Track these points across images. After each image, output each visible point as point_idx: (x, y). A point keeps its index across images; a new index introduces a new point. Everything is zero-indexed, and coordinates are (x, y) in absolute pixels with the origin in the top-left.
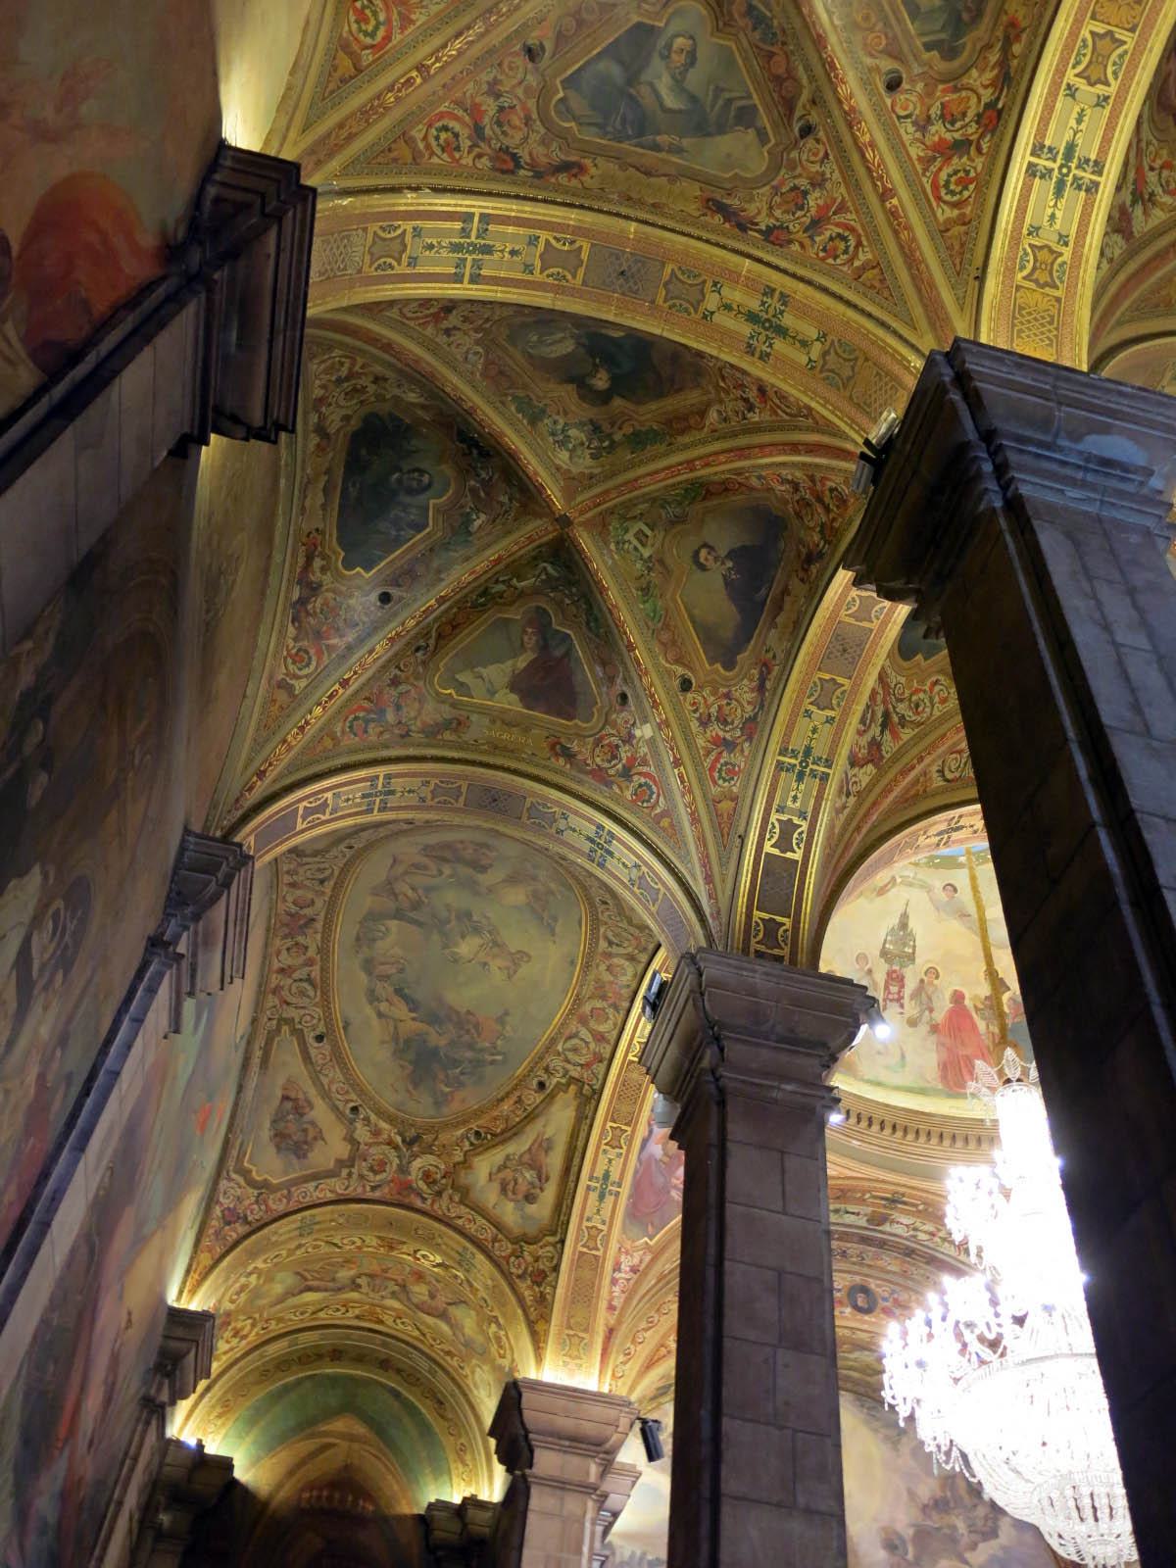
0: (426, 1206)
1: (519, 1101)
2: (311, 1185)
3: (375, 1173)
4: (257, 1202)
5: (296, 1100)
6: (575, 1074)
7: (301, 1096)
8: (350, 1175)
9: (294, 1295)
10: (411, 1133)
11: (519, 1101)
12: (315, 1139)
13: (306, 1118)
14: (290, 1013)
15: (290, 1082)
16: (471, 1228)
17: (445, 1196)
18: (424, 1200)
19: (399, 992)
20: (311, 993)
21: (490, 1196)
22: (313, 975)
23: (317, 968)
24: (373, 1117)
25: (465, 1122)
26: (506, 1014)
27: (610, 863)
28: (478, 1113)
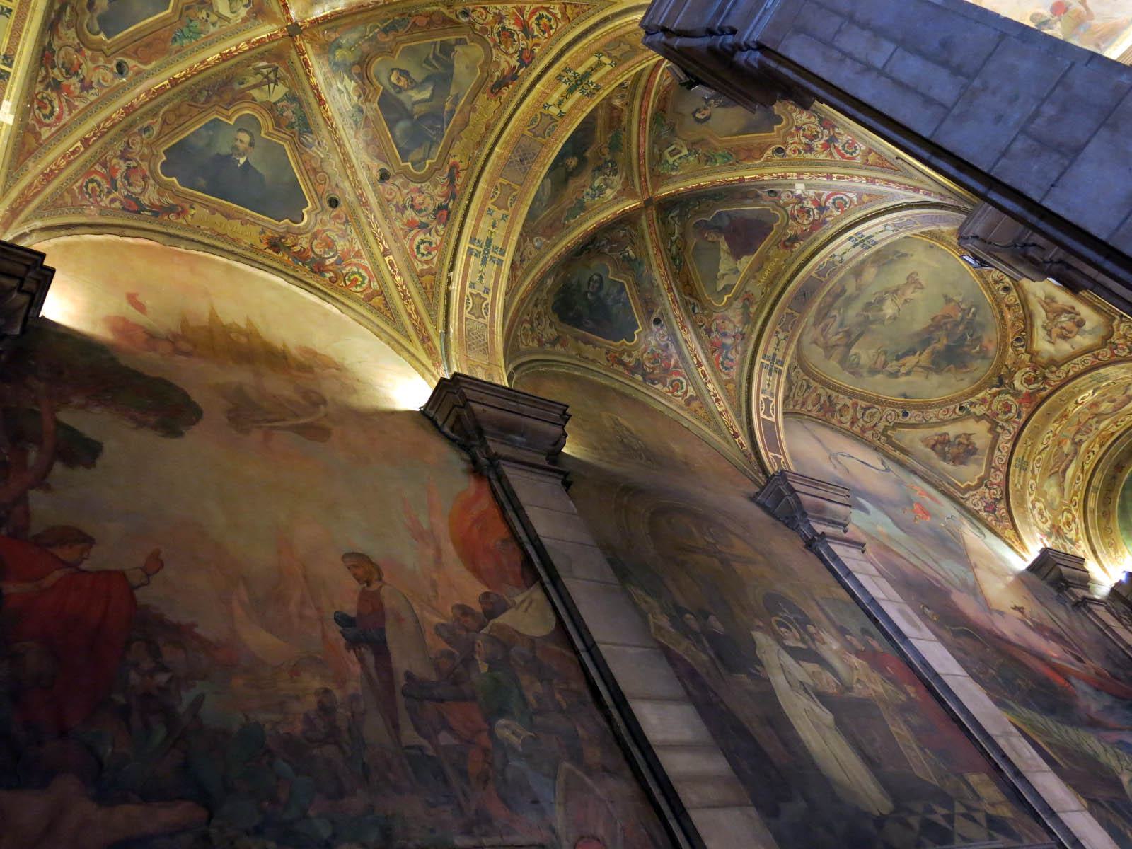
0: (1049, 389)
1: (1009, 307)
2: (997, 453)
3: (1010, 411)
4: (990, 489)
5: (937, 442)
7: (936, 438)
8: (1002, 427)
9: (1064, 481)
10: (995, 380)
11: (1009, 307)
13: (952, 440)
14: (881, 426)
15: (924, 441)
16: (1080, 368)
17: (1049, 375)
18: (1044, 389)
19: (898, 358)
21: (1065, 347)
22: (863, 406)
24: (972, 399)
25: (1005, 346)
27: (876, 238)
28: (1004, 336)
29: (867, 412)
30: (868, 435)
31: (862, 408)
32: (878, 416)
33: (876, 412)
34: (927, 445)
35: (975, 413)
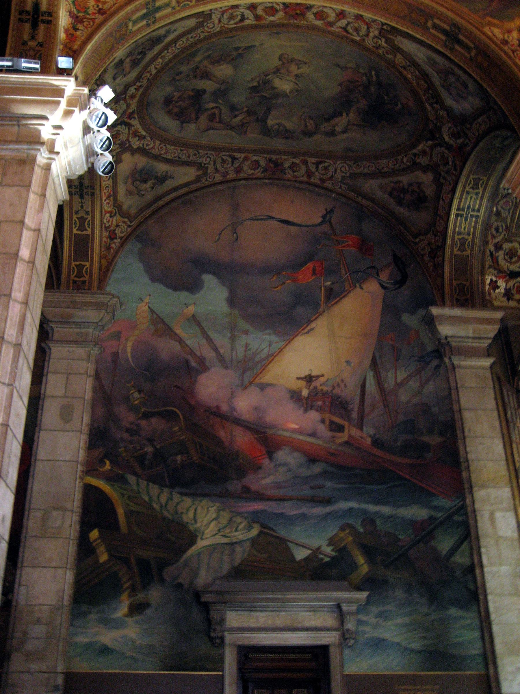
4: (435, 236)
5: (394, 189)
6: (377, 33)
8: (444, 178)
11: (405, 68)
12: (419, 187)
13: (406, 187)
14: (339, 176)
15: (381, 187)
19: (328, 120)
20: (326, 164)
23: (309, 159)
24: (414, 151)
26: (338, 66)
29: (320, 166)
30: (328, 184)
31: (313, 163)
32: (331, 169)
33: (329, 166)
34: (384, 192)
35: (419, 163)
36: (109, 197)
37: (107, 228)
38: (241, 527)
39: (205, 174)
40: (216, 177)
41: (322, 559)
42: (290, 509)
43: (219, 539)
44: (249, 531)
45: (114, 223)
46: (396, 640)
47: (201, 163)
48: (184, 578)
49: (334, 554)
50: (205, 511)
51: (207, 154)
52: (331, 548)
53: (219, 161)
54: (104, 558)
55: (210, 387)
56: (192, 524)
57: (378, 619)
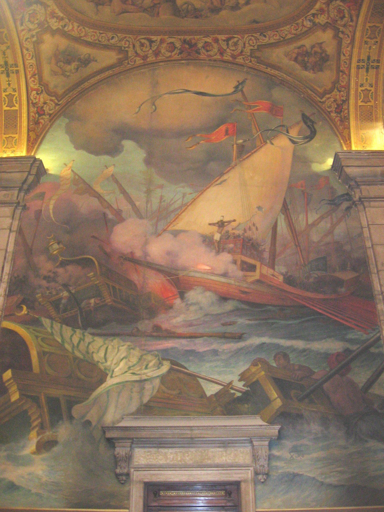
2: (343, 58)
3: (344, 17)
4: (340, 91)
5: (298, 54)
7: (296, 51)
8: (343, 32)
12: (321, 48)
13: (309, 50)
14: (248, 50)
20: (236, 40)
22: (224, 38)
23: (219, 37)
24: (313, 11)
29: (230, 43)
30: (240, 60)
31: (224, 41)
32: (241, 44)
33: (238, 41)
34: (290, 59)
35: (319, 23)
36: (34, 75)
37: (34, 104)
38: (151, 364)
39: (127, 58)
40: (137, 60)
41: (234, 394)
42: (200, 346)
43: (129, 377)
44: (159, 368)
45: (42, 100)
46: (311, 475)
47: (121, 47)
48: (92, 416)
49: (246, 388)
50: (116, 350)
51: (125, 37)
52: (243, 383)
53: (137, 44)
54: (15, 397)
55: (125, 237)
56: (102, 363)
57: (292, 454)
